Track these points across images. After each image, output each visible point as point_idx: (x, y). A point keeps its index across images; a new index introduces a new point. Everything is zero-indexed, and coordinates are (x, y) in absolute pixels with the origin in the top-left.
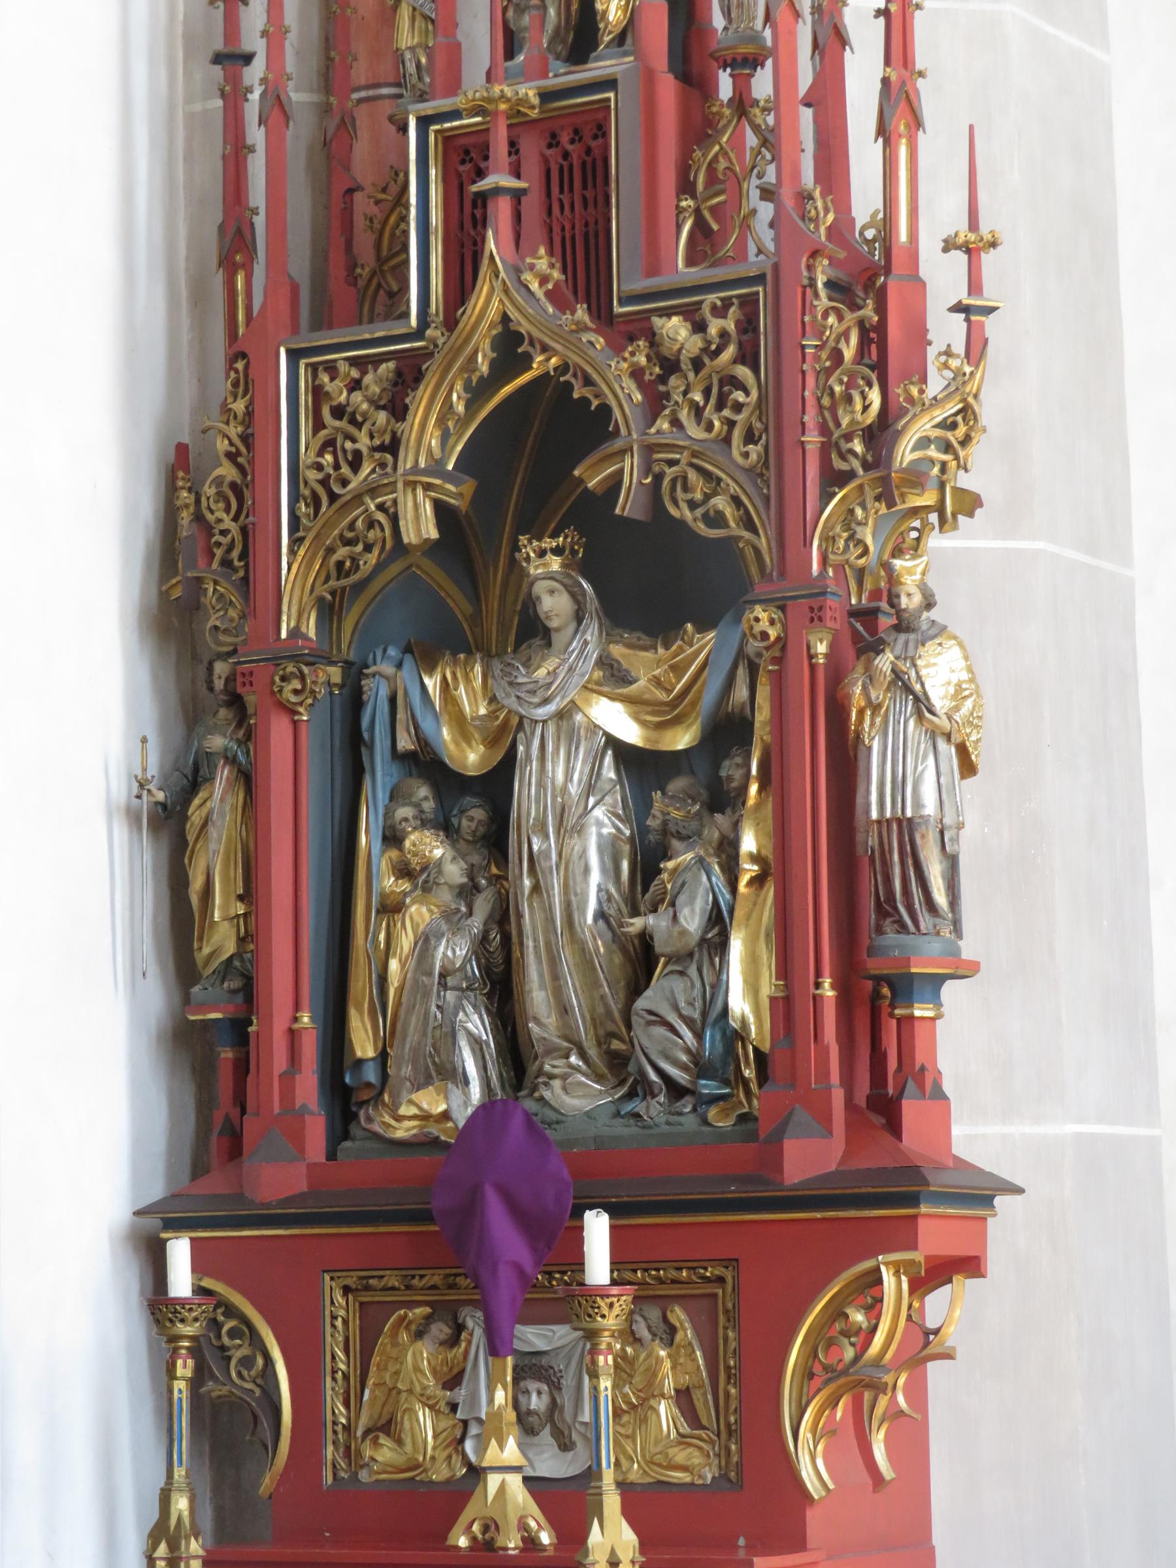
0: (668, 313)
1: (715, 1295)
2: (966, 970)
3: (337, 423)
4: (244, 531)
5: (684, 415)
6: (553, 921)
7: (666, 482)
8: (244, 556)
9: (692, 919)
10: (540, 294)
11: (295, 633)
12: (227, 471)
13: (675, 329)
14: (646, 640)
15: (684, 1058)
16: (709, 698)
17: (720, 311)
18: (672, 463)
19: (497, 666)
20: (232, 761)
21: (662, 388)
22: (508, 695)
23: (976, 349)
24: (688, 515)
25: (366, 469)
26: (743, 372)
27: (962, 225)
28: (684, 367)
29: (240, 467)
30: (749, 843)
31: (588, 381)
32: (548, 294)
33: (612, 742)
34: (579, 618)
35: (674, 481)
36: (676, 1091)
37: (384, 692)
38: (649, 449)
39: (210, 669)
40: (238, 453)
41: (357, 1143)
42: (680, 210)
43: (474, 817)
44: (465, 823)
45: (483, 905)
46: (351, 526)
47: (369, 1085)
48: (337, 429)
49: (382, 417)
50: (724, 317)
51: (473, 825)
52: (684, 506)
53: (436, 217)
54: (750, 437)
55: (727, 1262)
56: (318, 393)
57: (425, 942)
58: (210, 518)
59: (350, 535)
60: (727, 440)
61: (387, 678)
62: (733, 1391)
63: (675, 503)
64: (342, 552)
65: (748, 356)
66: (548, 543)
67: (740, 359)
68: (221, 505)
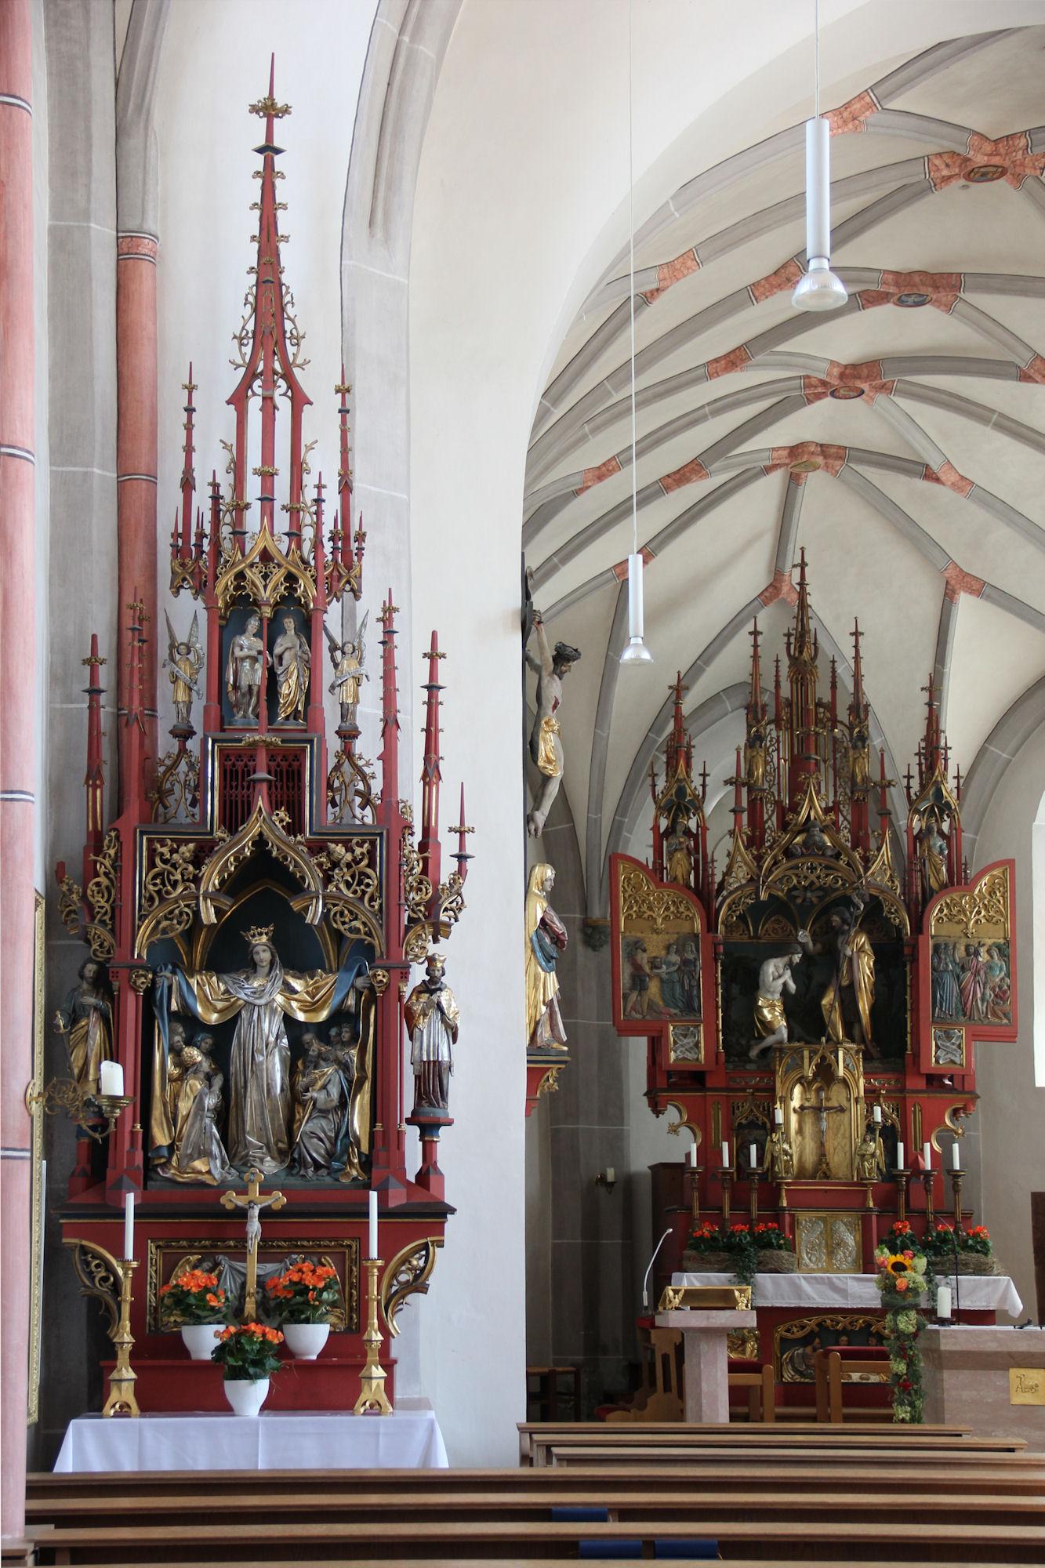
0: (337, 842)
1: (344, 1253)
2: (450, 1123)
3: (164, 866)
4: (113, 909)
5: (342, 886)
6: (263, 1091)
7: (332, 913)
8: (112, 918)
9: (335, 1093)
10: (280, 826)
11: (139, 955)
12: (102, 879)
14: (298, 974)
15: (323, 1152)
16: (335, 1001)
17: (360, 845)
18: (335, 905)
19: (225, 977)
20: (96, 1008)
21: (330, 873)
22: (240, 993)
23: (461, 872)
24: (342, 928)
25: (180, 889)
26: (369, 871)
27: (458, 825)
28: (342, 865)
29: (110, 879)
31: (297, 865)
32: (283, 827)
34: (272, 964)
35: (335, 914)
36: (317, 1166)
37: (166, 984)
38: (324, 898)
39: (84, 967)
40: (110, 873)
41: (158, 1183)
42: (328, 796)
43: (208, 1042)
44: (203, 1044)
45: (218, 1081)
46: (171, 912)
47: (163, 1157)
48: (165, 869)
49: (191, 868)
50: (362, 847)
51: (207, 1046)
52: (339, 923)
53: (217, 783)
54: (372, 899)
55: (353, 1239)
56: (152, 852)
57: (199, 1100)
58: (91, 899)
59: (170, 916)
60: (361, 899)
61: (168, 978)
62: (355, 1292)
63: (336, 922)
64: (165, 923)
65: (371, 865)
66: (264, 930)
67: (368, 866)
68: (100, 895)
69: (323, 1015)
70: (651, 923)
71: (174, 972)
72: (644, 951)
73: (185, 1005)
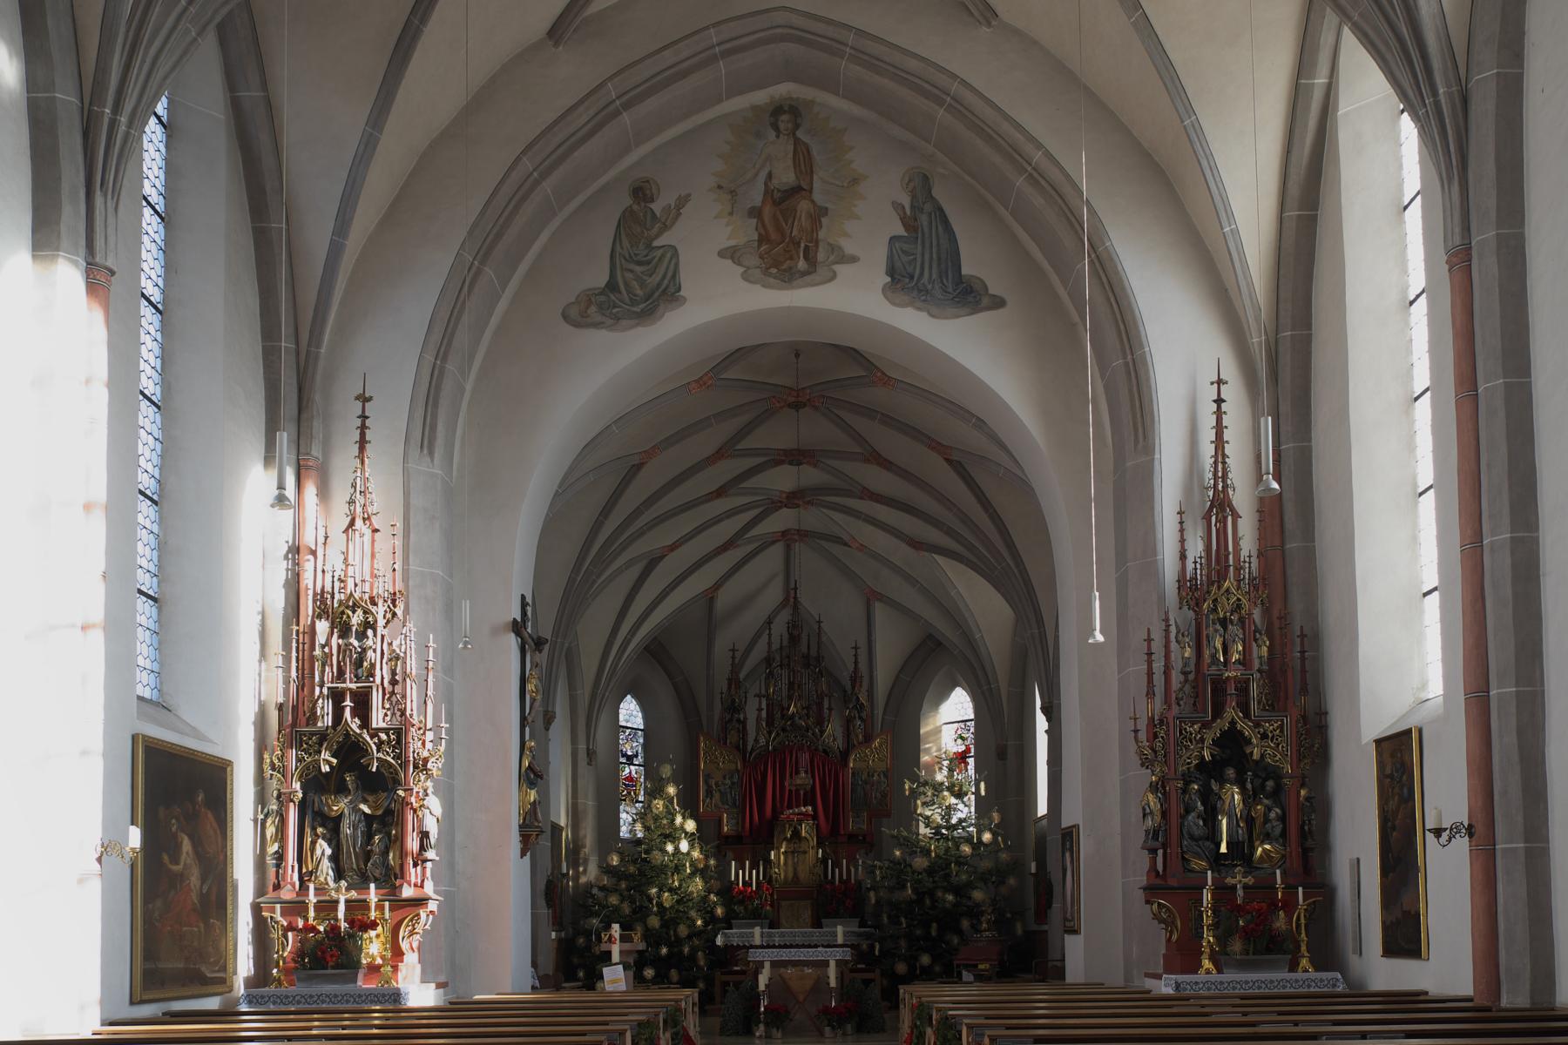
4: (283, 766)
12: (279, 752)
13: (383, 736)
26: (397, 746)
30: (394, 832)
33: (364, 812)
69: (380, 812)
70: (716, 765)
71: (315, 794)
72: (713, 778)
73: (320, 809)
